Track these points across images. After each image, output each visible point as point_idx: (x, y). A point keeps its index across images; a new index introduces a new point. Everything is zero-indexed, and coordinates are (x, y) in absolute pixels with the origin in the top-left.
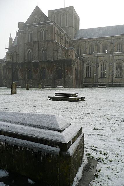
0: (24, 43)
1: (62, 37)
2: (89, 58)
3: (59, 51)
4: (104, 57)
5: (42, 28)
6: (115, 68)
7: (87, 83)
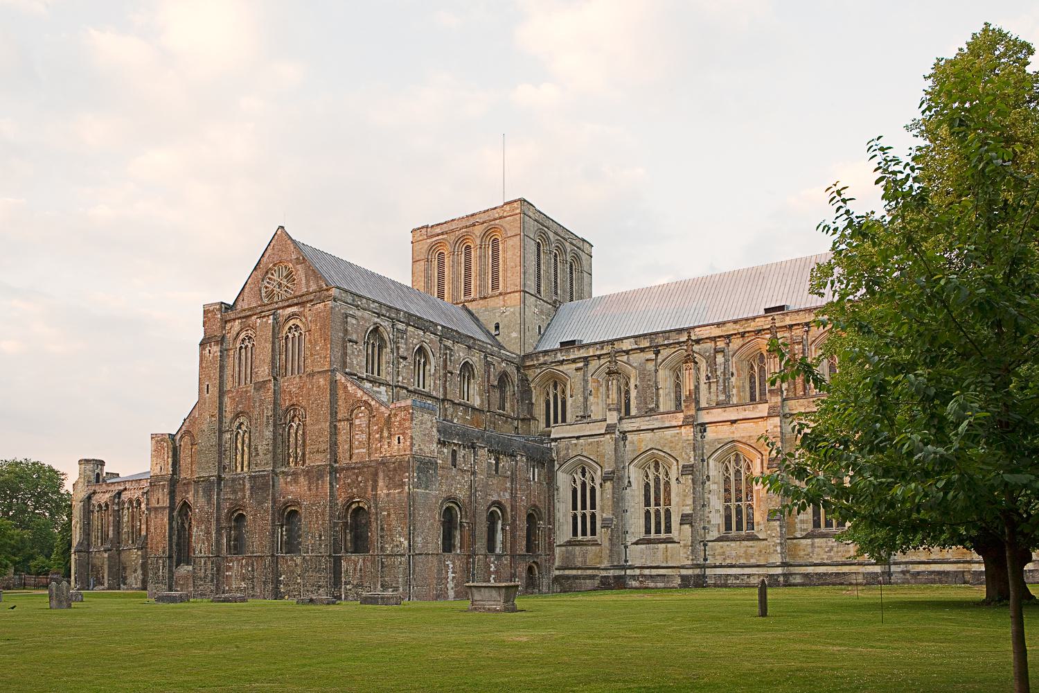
0: (222, 393)
1: (421, 350)
2: (581, 441)
3: (357, 422)
4: (658, 433)
5: (291, 323)
6: (714, 487)
7: (574, 572)
